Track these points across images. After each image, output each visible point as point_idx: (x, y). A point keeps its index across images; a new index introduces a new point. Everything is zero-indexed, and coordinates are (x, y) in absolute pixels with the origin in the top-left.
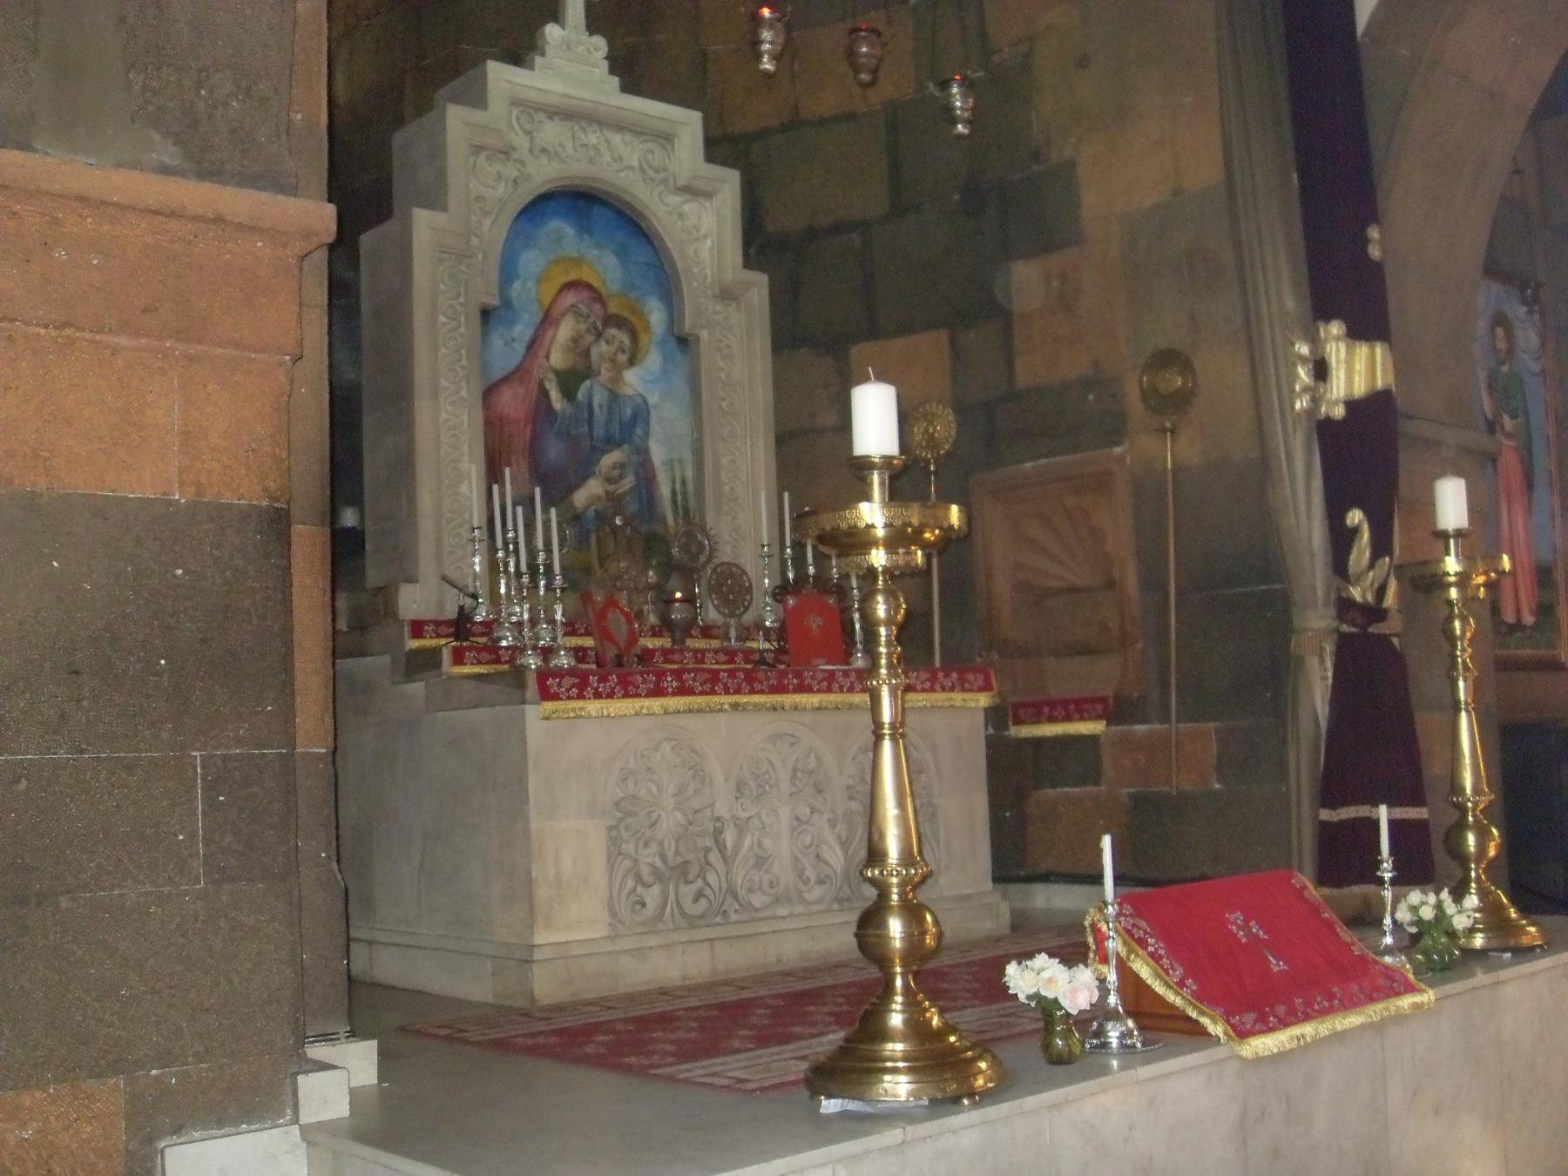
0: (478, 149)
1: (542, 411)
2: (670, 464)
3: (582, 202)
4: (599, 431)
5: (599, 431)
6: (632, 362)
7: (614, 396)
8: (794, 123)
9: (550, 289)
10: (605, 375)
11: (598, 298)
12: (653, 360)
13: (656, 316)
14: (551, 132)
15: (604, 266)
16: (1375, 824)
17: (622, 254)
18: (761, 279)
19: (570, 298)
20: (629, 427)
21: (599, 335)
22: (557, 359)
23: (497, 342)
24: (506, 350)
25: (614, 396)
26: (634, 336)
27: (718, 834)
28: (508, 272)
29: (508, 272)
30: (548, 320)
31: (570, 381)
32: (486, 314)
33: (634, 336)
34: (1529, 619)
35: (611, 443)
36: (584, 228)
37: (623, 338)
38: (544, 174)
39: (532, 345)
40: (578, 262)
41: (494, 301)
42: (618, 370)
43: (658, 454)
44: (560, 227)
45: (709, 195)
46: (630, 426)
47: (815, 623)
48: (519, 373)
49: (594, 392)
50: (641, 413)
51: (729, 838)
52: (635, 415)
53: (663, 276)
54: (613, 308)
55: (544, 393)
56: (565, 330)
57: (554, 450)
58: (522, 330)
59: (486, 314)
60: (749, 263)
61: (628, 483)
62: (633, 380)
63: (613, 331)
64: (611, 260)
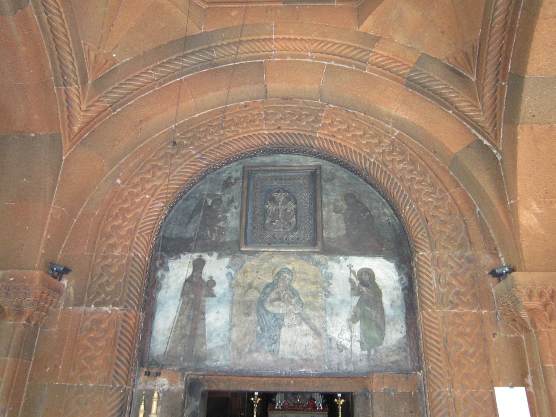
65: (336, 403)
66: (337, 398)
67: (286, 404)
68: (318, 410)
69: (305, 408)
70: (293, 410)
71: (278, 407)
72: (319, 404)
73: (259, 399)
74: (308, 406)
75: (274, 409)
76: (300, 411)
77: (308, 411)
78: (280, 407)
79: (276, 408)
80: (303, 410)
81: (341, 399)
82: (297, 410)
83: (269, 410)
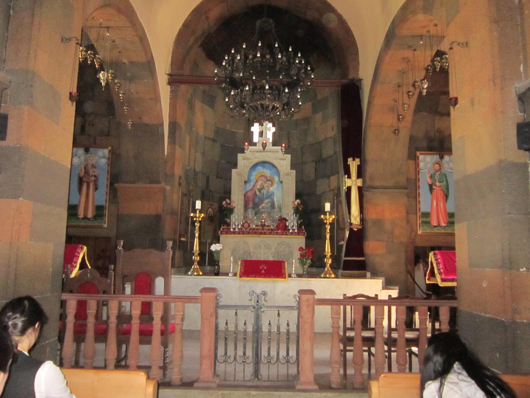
0: (244, 159)
1: (255, 194)
2: (278, 201)
3: (264, 163)
4: (265, 196)
5: (265, 196)
6: (271, 186)
7: (268, 192)
8: (326, 139)
9: (258, 177)
10: (266, 188)
11: (266, 177)
12: (275, 185)
13: (276, 179)
14: (257, 154)
15: (267, 172)
16: (345, 261)
17: (270, 170)
18: (294, 172)
19: (261, 178)
20: (270, 196)
21: (266, 183)
22: (258, 187)
23: (248, 185)
24: (249, 187)
25: (268, 192)
26: (272, 182)
27: (250, 254)
28: (249, 175)
29: (249, 175)
30: (257, 181)
31: (260, 190)
32: (246, 182)
33: (272, 182)
34: (443, 224)
35: (267, 198)
36: (264, 167)
37: (270, 183)
38: (256, 161)
39: (254, 186)
40: (263, 172)
41: (247, 180)
42: (269, 188)
43: (275, 200)
44: (260, 169)
45: (285, 159)
46: (270, 196)
47: (281, 225)
48: (252, 189)
49: (264, 191)
50: (273, 194)
51: (252, 254)
52: (271, 195)
53: (278, 173)
54: (268, 178)
55: (255, 192)
56: (260, 183)
57: (257, 200)
58: (252, 184)
59: (246, 182)
60: (291, 169)
61: (270, 204)
62: (271, 189)
63: (268, 182)
64: (268, 171)
65: (322, 220)
66: (325, 213)
67: (246, 225)
68: (292, 233)
69: (272, 230)
70: (256, 233)
71: (234, 229)
72: (293, 226)
73: (203, 215)
74: (278, 227)
75: (228, 232)
76: (265, 234)
77: (277, 234)
78: (237, 230)
79: (232, 230)
80: (270, 233)
81: (331, 213)
82: (261, 234)
83: (221, 234)
